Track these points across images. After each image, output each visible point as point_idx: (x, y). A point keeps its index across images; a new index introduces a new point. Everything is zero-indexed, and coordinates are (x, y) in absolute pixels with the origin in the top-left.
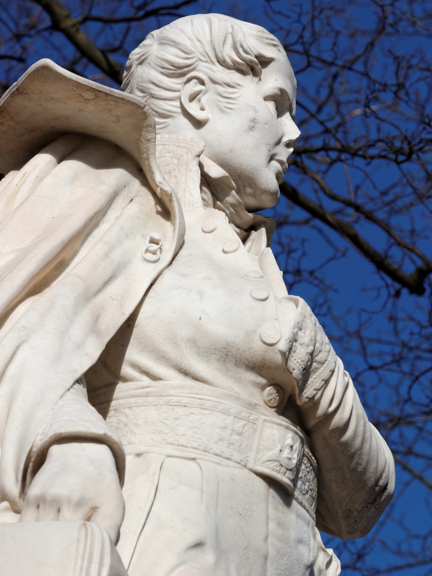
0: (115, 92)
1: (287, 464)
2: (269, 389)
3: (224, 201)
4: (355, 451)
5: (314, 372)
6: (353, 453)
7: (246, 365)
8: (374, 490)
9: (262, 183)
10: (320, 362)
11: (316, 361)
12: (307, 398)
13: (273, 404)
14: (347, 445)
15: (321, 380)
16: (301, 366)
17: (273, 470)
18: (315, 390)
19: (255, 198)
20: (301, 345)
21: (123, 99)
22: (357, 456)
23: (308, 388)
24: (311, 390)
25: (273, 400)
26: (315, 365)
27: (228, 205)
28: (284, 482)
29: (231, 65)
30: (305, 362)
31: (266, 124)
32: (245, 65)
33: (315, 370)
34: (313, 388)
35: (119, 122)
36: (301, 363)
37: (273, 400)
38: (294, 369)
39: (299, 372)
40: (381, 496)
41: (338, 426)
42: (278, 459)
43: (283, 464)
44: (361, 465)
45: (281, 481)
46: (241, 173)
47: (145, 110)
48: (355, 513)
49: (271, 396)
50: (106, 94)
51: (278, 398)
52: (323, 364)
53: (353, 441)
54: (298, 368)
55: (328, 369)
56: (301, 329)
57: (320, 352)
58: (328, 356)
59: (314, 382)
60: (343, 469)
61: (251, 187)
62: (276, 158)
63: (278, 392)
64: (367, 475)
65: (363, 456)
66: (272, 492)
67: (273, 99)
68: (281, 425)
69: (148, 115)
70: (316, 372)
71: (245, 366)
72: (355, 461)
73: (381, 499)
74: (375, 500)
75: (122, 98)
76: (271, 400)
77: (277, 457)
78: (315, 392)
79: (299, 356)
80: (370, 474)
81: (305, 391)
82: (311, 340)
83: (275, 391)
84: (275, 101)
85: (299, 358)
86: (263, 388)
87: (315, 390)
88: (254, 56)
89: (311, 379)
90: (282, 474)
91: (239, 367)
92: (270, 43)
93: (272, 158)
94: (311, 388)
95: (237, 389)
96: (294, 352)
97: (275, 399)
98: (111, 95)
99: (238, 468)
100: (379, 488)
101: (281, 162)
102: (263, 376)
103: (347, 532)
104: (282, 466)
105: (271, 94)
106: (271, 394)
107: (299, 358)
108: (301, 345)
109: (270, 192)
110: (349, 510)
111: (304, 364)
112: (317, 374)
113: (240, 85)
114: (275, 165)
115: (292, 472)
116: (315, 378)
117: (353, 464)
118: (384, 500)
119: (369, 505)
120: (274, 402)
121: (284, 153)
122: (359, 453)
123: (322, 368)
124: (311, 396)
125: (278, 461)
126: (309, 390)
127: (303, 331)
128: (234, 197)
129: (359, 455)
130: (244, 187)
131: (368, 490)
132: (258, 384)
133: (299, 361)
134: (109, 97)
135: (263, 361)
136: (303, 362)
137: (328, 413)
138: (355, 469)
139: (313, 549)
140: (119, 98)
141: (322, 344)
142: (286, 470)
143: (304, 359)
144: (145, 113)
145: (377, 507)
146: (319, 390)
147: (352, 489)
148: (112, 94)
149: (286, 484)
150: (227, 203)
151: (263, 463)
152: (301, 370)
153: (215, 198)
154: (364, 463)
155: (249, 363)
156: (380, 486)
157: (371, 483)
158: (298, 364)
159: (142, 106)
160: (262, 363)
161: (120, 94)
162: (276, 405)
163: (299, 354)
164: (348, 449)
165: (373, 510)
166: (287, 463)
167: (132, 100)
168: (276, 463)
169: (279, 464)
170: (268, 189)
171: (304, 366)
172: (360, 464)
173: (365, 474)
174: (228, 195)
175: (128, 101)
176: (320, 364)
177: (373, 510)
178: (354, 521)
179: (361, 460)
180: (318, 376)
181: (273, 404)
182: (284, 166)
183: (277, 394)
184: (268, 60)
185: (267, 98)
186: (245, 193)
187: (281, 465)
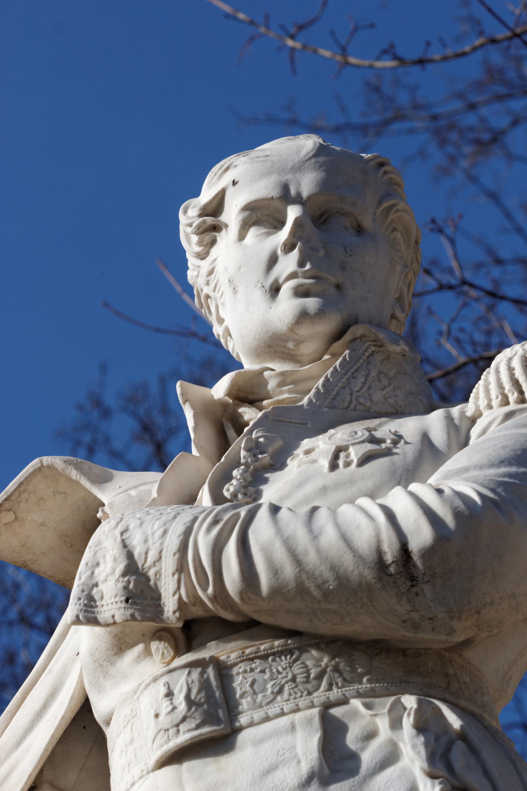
0: (9, 489)
1: (172, 721)
2: (155, 645)
3: (271, 392)
4: (296, 582)
5: (158, 580)
6: (296, 587)
7: (115, 654)
8: (391, 575)
9: (281, 327)
10: (154, 563)
11: (150, 568)
12: (174, 612)
13: (170, 655)
14: (277, 591)
15: (171, 576)
16: (119, 603)
17: (161, 746)
18: (174, 595)
19: (303, 342)
20: (106, 580)
21: (21, 484)
22: (306, 583)
23: (166, 604)
24: (171, 599)
25: (165, 652)
26: (151, 573)
27: (278, 391)
28: (181, 744)
29: (203, 250)
30: (121, 592)
31: (240, 268)
32: (202, 236)
33: (158, 576)
34: (171, 595)
35: (65, 493)
36: (117, 599)
37: (165, 652)
38: (113, 616)
39: (122, 611)
40: (414, 565)
41: (238, 590)
42: (158, 729)
43: (166, 727)
44: (328, 582)
45: (176, 746)
46: (265, 343)
47: (45, 464)
48: (415, 615)
49: (159, 651)
50: (6, 500)
51: (166, 644)
52: (160, 558)
53: (278, 579)
54: (116, 609)
55: (170, 556)
56: (98, 564)
57: (146, 553)
58: (162, 544)
59: (167, 589)
60: (318, 609)
61: (287, 341)
62: (281, 281)
63: (160, 639)
64: (354, 578)
65: (317, 572)
66: (187, 765)
67: (247, 226)
68: (149, 685)
69: (52, 465)
70: (160, 576)
71: (116, 656)
72: (312, 588)
73: (418, 569)
74: (413, 579)
75: (19, 485)
76: (163, 654)
77: (156, 727)
78: (177, 596)
79: (109, 595)
80: (356, 572)
81: (166, 609)
82: (115, 560)
83: (158, 642)
84: (256, 223)
85: (111, 598)
86: (148, 653)
87: (174, 595)
88: (197, 218)
89: (162, 591)
90: (174, 738)
91: (114, 664)
92: (220, 175)
93: (275, 290)
94: (168, 599)
95: (127, 687)
96: (102, 598)
97: (166, 648)
98: (10, 496)
99: (146, 779)
100: (393, 565)
101: (293, 276)
102: (135, 644)
103: (448, 635)
104: (167, 730)
105: (239, 227)
106: (157, 649)
107: (111, 598)
108: (106, 580)
109: (295, 324)
110: (404, 622)
111: (121, 596)
112: (163, 577)
113: (215, 260)
114: (286, 288)
115: (188, 720)
116: (165, 584)
117: (316, 593)
118: (424, 563)
119: (414, 590)
120: (168, 652)
121: (289, 263)
122: (305, 577)
123: (163, 564)
124: (176, 607)
125: (160, 731)
126: (169, 603)
127: (102, 562)
128: (271, 377)
129: (308, 578)
130: (285, 347)
131: (378, 586)
132: (139, 657)
133: (113, 600)
134: (13, 498)
135: (112, 635)
136: (118, 596)
137: (211, 596)
138: (327, 594)
139: (305, 754)
140: (17, 488)
141: (146, 541)
142: (175, 729)
143: (116, 592)
144: (48, 467)
145: (426, 579)
146: (179, 588)
147: (362, 608)
148: (9, 494)
149: (191, 739)
150: (274, 391)
151: (152, 751)
152: (124, 605)
153: (258, 404)
154: (328, 575)
155: (113, 650)
156: (393, 562)
157: (370, 577)
158: (114, 604)
159: (39, 465)
160: (114, 637)
161: (14, 484)
162: (172, 653)
163: (107, 594)
164: (285, 591)
165: (427, 588)
166: (170, 719)
167: (28, 474)
168: (160, 735)
169: (164, 732)
170: (289, 325)
171: (123, 598)
172: (325, 582)
173: (348, 580)
174: (266, 383)
175: (26, 478)
176: (157, 564)
177: (427, 588)
178: (429, 621)
179: (319, 579)
180: (165, 577)
181: (170, 655)
182: (300, 275)
183: (162, 642)
184: (216, 201)
185: (242, 237)
186: (294, 350)
187: (165, 730)
